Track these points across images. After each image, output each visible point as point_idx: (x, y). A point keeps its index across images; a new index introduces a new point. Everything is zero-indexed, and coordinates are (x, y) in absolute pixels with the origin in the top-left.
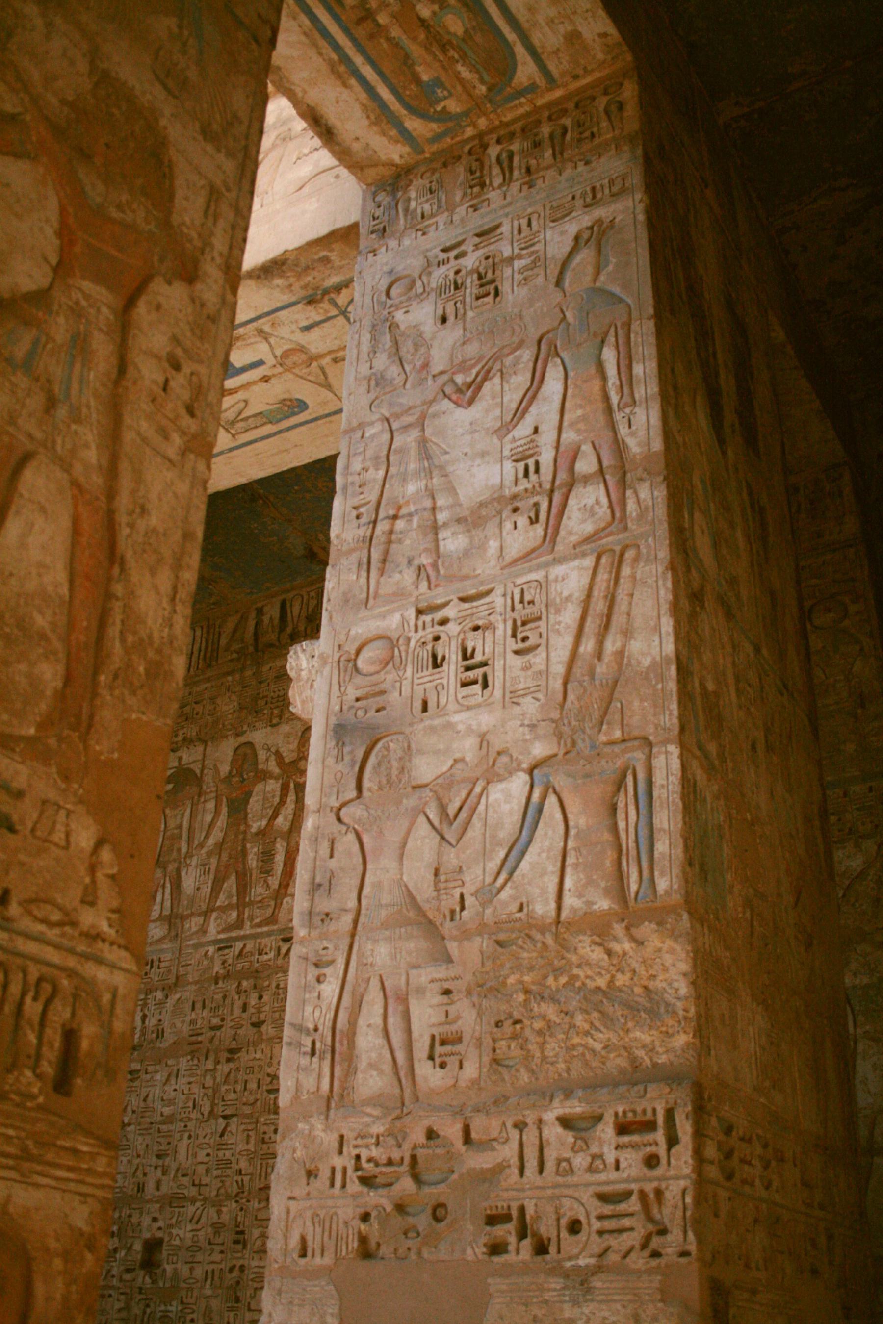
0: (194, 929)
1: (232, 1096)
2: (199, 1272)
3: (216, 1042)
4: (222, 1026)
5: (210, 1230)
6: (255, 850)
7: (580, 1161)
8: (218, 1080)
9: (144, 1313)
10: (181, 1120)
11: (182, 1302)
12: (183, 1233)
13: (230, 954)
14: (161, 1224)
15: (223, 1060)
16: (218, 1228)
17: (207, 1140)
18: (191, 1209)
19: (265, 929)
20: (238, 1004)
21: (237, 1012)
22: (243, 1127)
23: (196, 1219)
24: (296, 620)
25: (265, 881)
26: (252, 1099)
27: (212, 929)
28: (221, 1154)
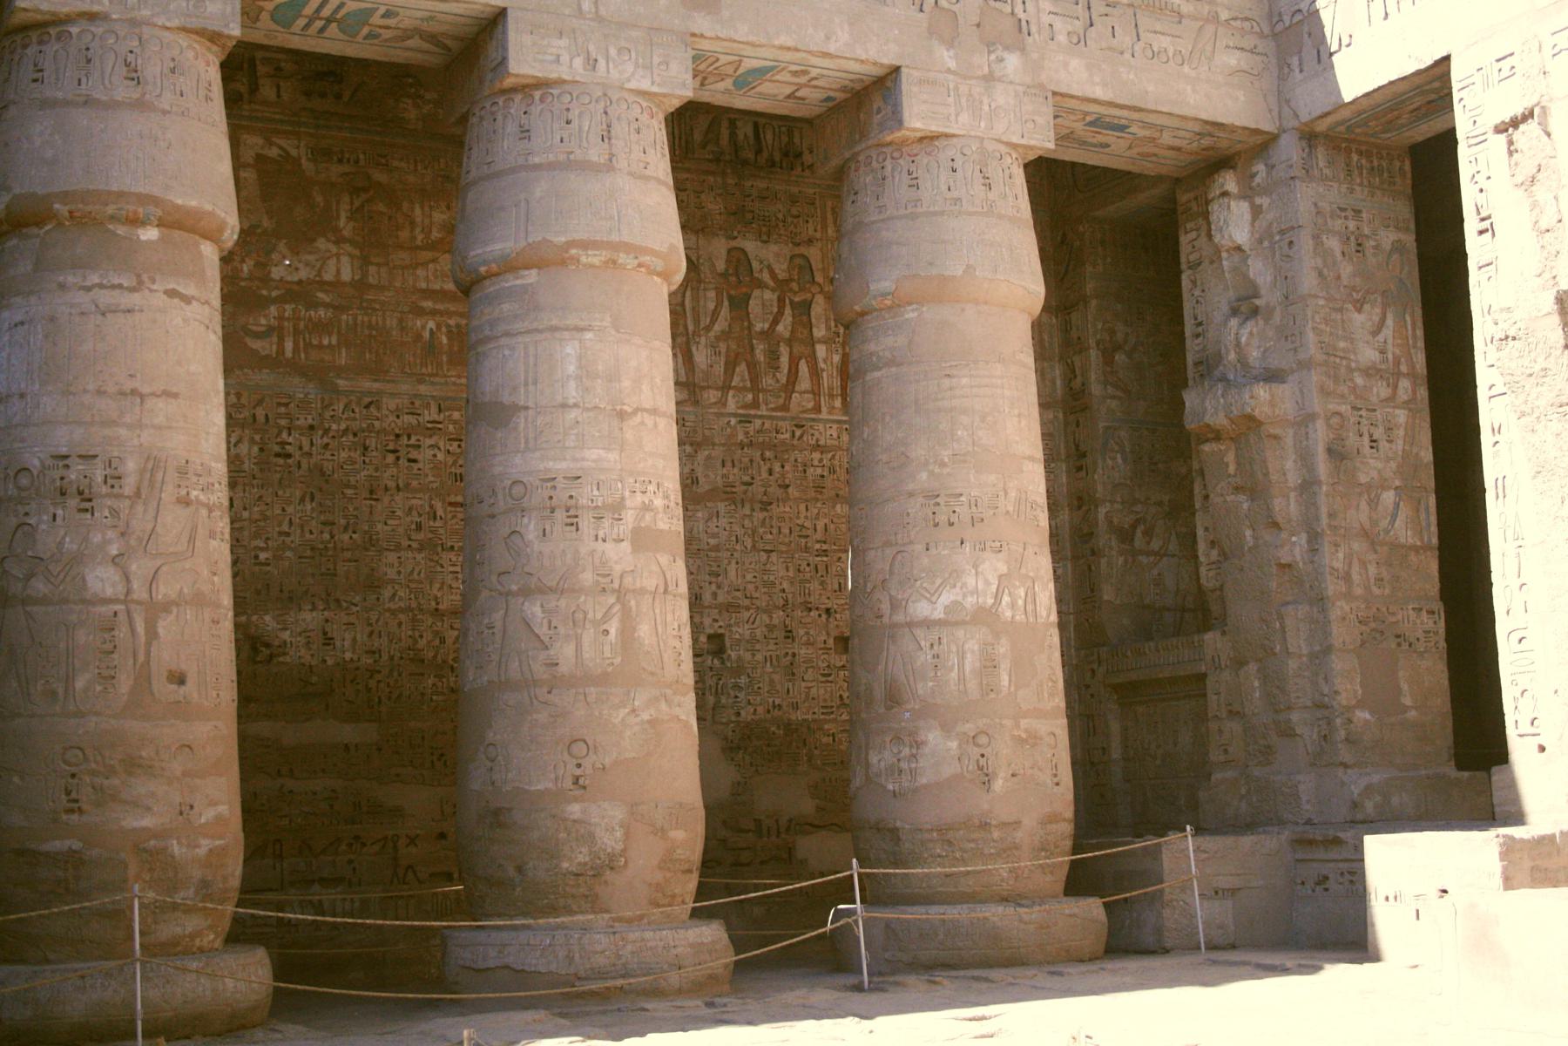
0: (713, 400)
1: (770, 537)
2: (759, 657)
3: (749, 494)
4: (752, 484)
5: (764, 629)
6: (762, 347)
7: (1418, 621)
8: (755, 523)
9: (717, 684)
10: (728, 550)
11: (749, 677)
12: (743, 631)
13: (751, 428)
14: (721, 623)
15: (757, 509)
16: (771, 628)
17: (753, 566)
18: (746, 615)
19: (779, 414)
20: (764, 469)
21: (765, 475)
22: (782, 560)
23: (752, 620)
24: (770, 147)
25: (774, 376)
26: (787, 540)
27: (732, 405)
28: (766, 578)
